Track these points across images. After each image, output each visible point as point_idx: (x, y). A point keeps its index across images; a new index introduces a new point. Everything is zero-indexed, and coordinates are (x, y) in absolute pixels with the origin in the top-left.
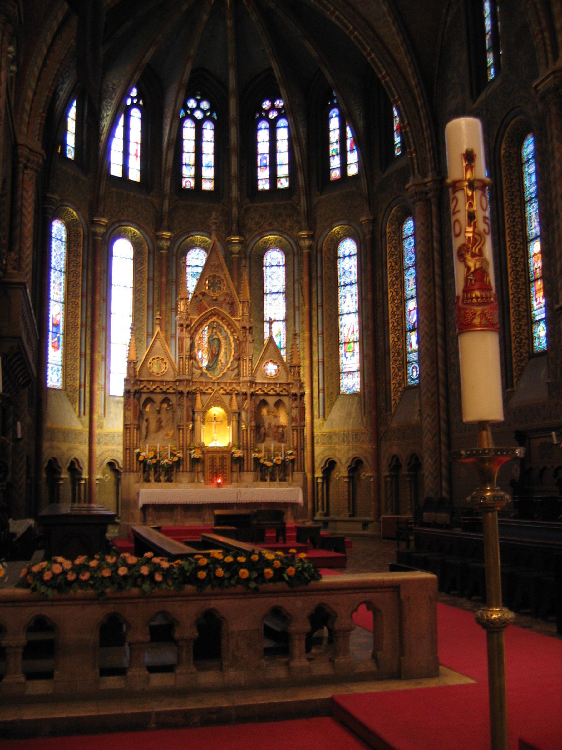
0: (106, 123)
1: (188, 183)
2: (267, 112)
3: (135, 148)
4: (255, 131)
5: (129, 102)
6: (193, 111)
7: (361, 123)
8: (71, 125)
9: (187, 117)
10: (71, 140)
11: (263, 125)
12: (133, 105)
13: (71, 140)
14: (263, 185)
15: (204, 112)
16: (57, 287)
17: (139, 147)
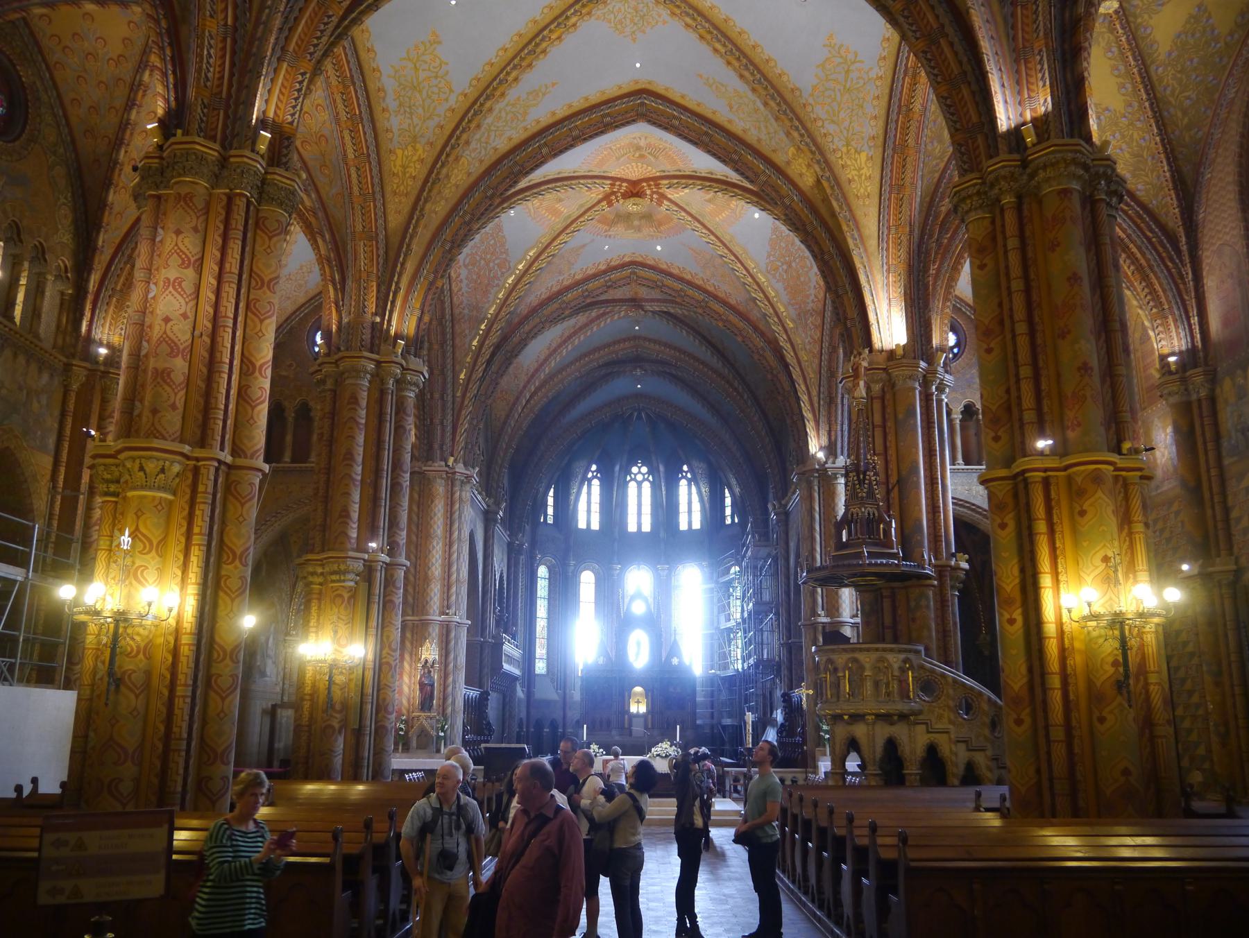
0: (572, 498)
1: (632, 527)
2: (686, 472)
3: (596, 507)
4: (677, 486)
5: (590, 475)
6: (635, 475)
7: (737, 490)
8: (550, 501)
9: (632, 480)
10: (550, 511)
11: (683, 483)
12: (594, 477)
13: (550, 511)
14: (683, 526)
15: (644, 475)
16: (542, 608)
17: (598, 506)
